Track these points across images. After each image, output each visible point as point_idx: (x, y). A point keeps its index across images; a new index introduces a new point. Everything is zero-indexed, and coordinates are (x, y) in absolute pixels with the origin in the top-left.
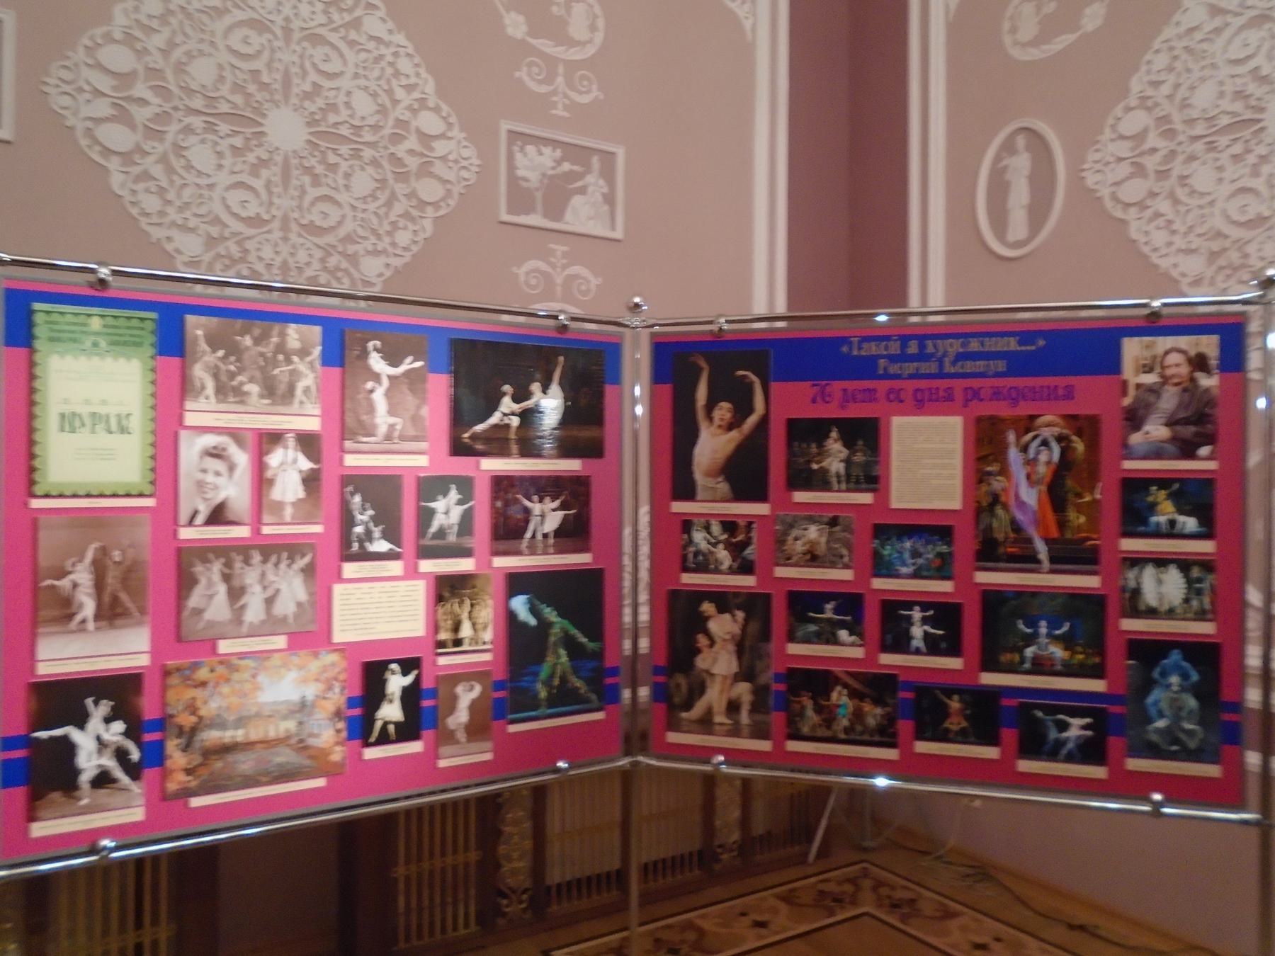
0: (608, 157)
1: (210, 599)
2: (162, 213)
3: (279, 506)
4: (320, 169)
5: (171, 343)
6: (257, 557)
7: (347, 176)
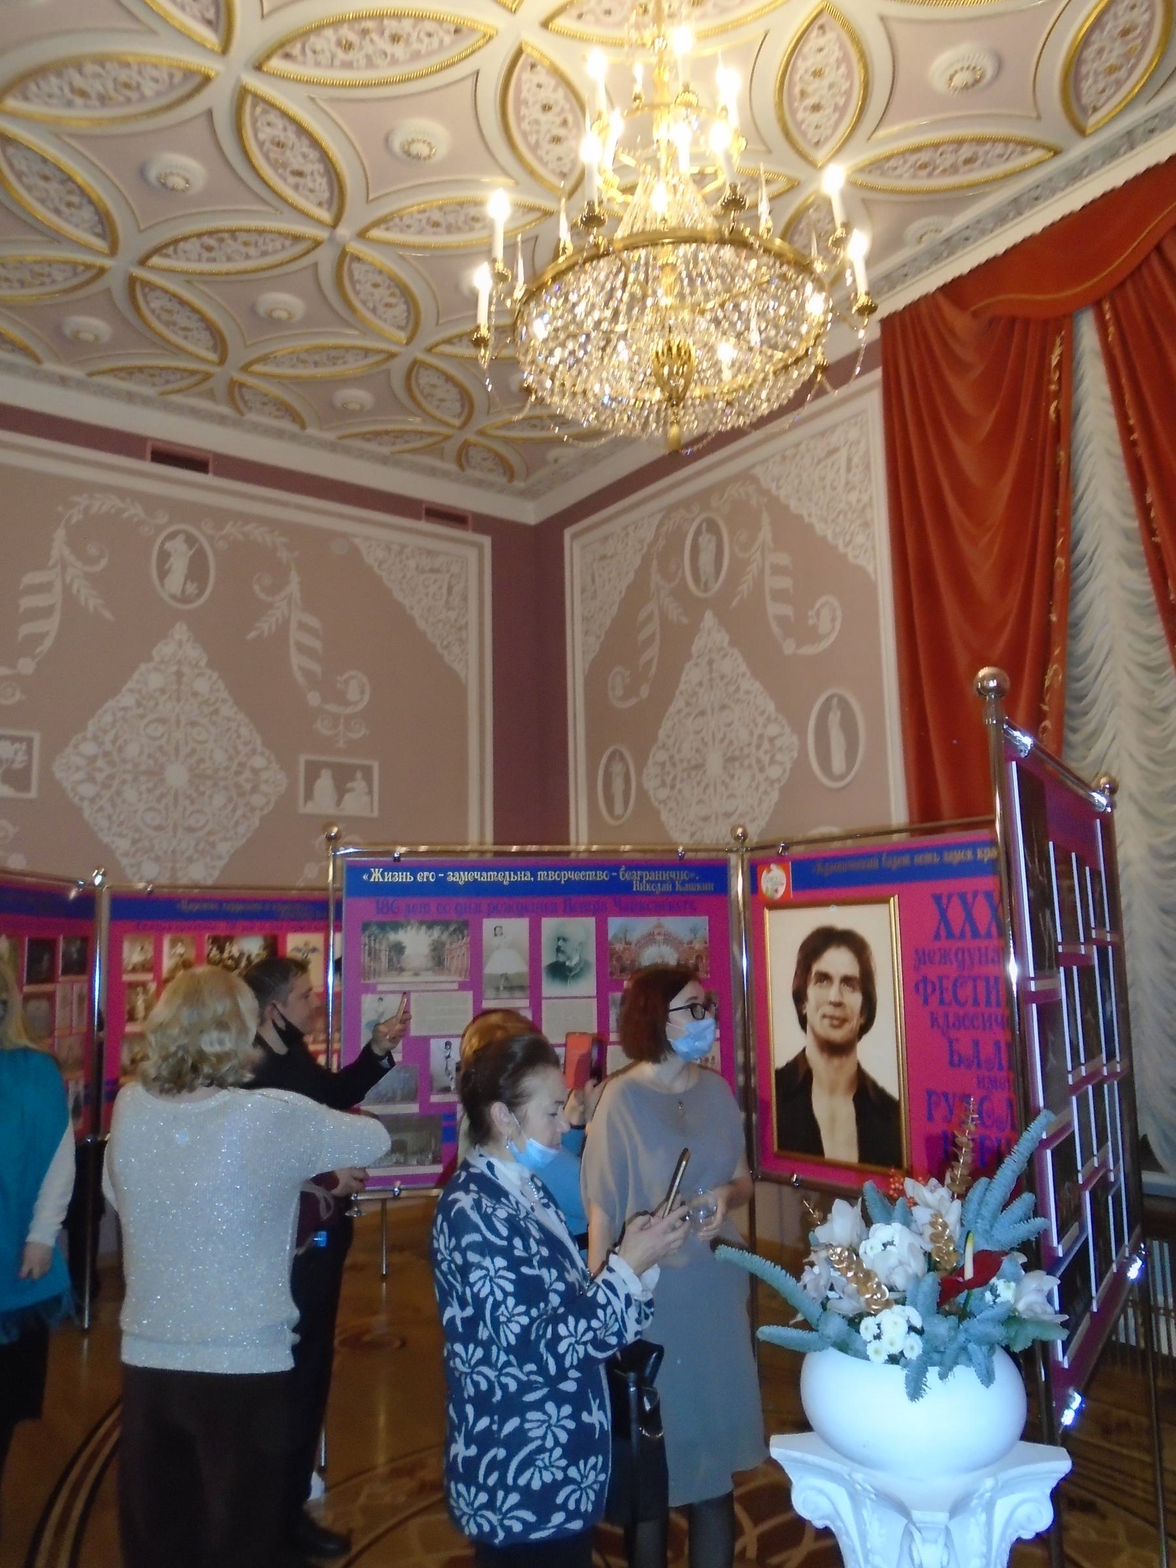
0: (367, 772)
2: (109, 829)
4: (194, 795)
7: (211, 797)
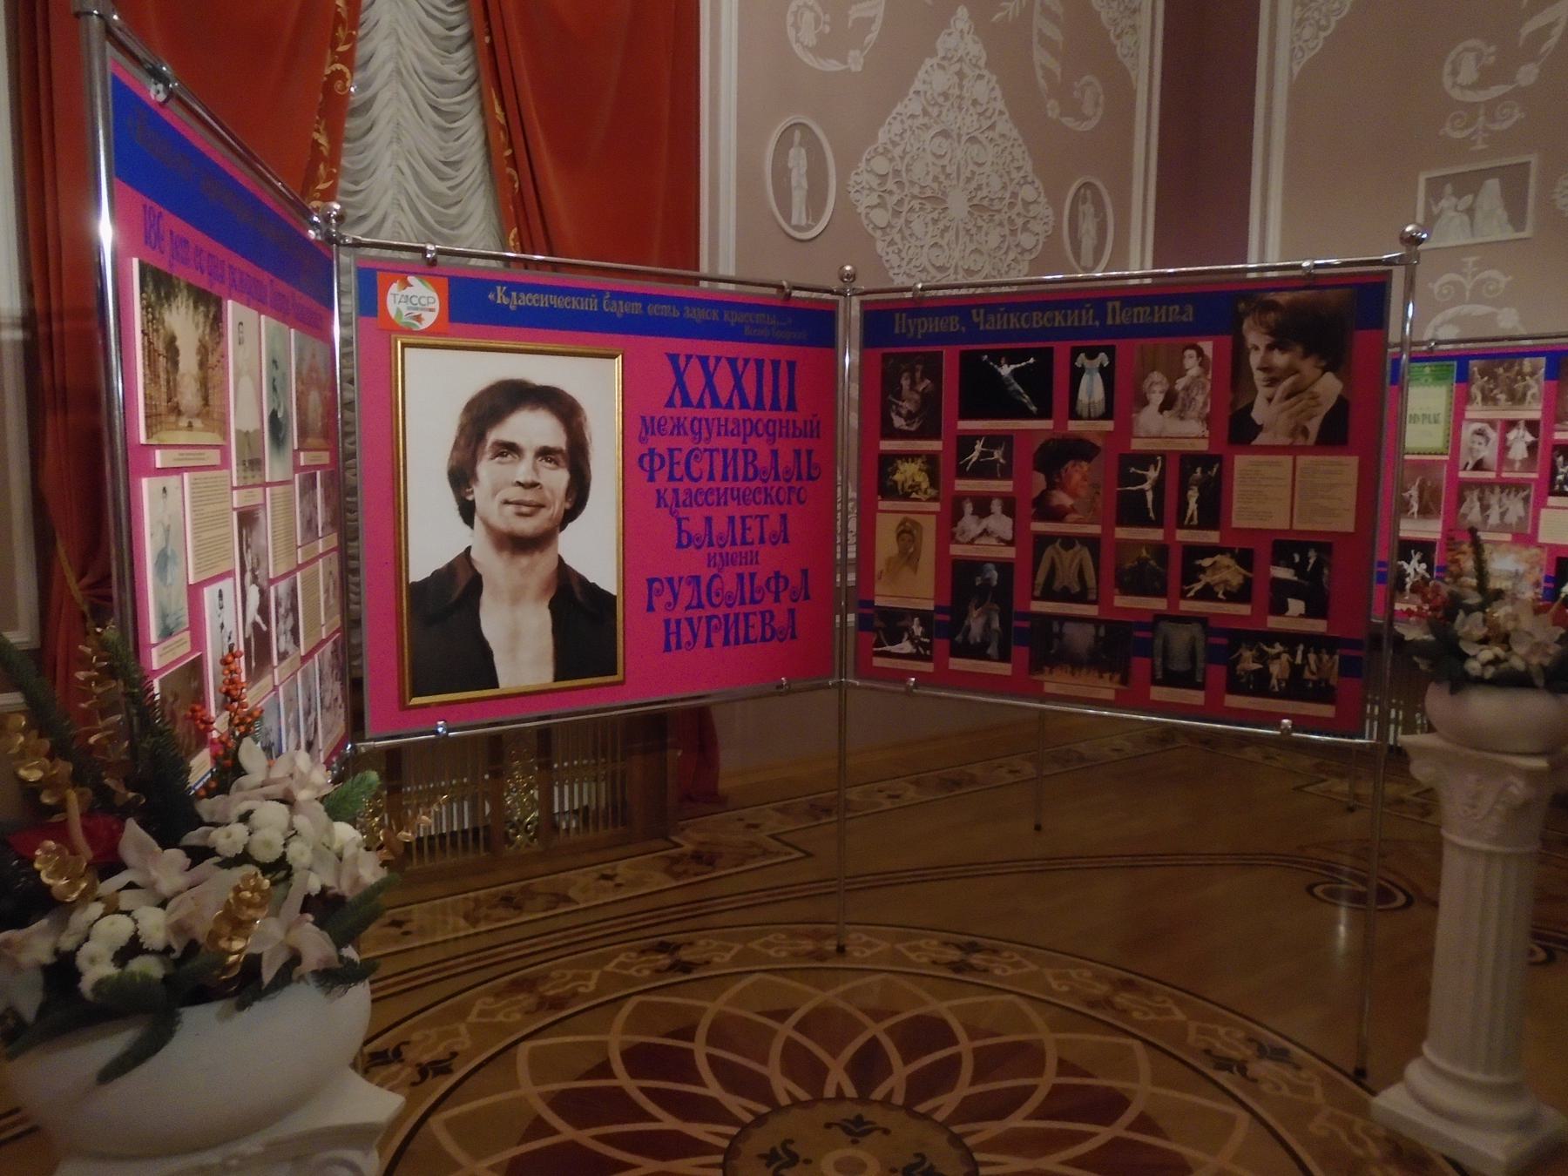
1: (1472, 511)
3: (1512, 462)
5: (1463, 377)
6: (1497, 490)
